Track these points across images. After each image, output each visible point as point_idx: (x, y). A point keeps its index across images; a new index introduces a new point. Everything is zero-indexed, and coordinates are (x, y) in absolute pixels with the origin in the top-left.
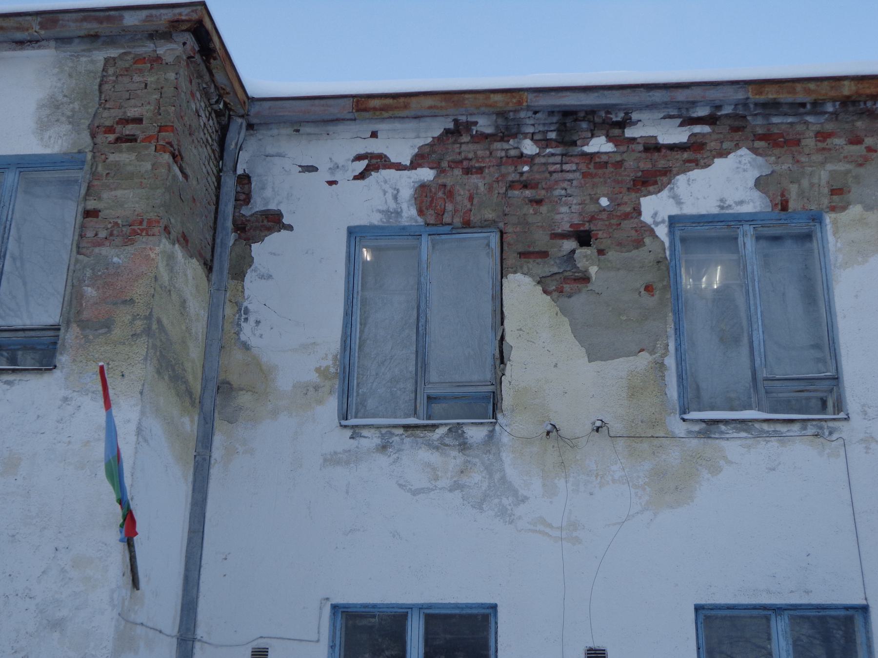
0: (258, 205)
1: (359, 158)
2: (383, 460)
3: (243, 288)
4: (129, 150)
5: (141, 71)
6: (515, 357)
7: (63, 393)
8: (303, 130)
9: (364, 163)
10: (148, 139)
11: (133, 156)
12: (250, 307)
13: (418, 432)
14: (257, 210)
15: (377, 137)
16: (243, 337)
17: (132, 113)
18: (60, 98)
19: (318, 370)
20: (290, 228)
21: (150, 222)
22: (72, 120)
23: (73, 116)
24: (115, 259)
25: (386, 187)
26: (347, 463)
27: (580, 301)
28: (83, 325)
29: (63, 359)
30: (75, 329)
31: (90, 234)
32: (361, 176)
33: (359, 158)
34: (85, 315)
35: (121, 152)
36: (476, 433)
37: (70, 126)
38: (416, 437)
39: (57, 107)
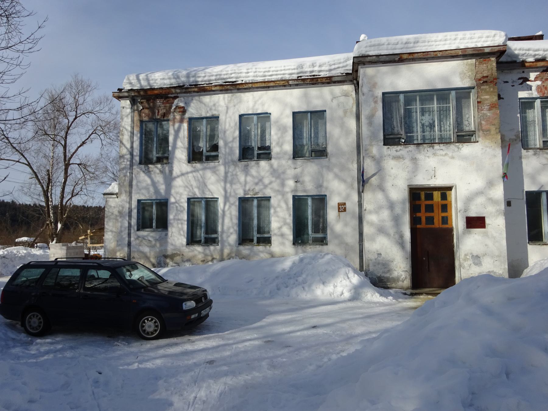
1: (520, 79)
2: (535, 157)
4: (487, 85)
7: (481, 147)
9: (521, 81)
10: (491, 82)
11: (488, 87)
13: (543, 150)
19: (515, 135)
20: (503, 99)
21: (495, 104)
24: (488, 114)
28: (483, 131)
29: (480, 139)
31: (480, 108)
32: (521, 84)
33: (520, 79)
35: (484, 86)
37: (469, 79)
38: (543, 151)
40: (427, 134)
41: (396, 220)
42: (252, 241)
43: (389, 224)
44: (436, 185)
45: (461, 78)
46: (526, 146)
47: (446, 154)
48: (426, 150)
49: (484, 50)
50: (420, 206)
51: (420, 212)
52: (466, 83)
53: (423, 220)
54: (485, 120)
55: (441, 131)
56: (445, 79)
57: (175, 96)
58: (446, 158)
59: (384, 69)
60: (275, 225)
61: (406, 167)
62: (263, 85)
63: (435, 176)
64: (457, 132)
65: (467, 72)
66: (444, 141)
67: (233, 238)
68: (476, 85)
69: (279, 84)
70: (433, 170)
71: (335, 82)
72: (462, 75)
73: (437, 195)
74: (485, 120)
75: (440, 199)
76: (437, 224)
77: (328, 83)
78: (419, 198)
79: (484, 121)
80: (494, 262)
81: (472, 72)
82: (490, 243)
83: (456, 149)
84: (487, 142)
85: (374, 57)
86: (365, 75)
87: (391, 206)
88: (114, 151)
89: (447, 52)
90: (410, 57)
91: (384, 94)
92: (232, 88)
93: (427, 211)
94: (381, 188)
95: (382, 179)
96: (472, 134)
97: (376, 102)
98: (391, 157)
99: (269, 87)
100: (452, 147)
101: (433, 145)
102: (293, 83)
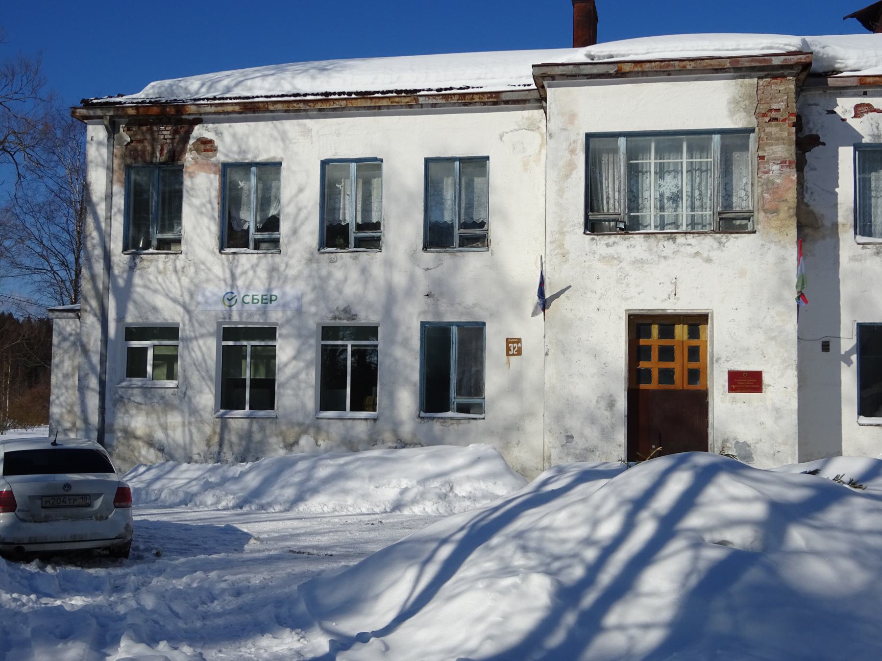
0: (806, 132)
3: (803, 175)
4: (776, 126)
5: (776, 84)
7: (761, 242)
8: (828, 91)
11: (778, 129)
12: (808, 185)
14: (807, 134)
15: (866, 95)
16: (805, 201)
17: (775, 106)
18: (738, 98)
20: (824, 144)
22: (745, 109)
23: (746, 108)
25: (872, 122)
26: (861, 260)
28: (766, 211)
29: (759, 227)
30: (762, 214)
34: (767, 207)
35: (772, 126)
37: (745, 114)
39: (737, 103)
40: (668, 213)
44: (676, 311)
45: (730, 110)
47: (697, 254)
48: (660, 244)
49: (771, 60)
50: (649, 348)
51: (649, 358)
52: (738, 122)
53: (655, 374)
54: (771, 191)
55: (693, 208)
57: (195, 119)
61: (623, 275)
63: (675, 295)
64: (719, 213)
65: (741, 99)
66: (695, 228)
68: (756, 126)
69: (398, 102)
70: (673, 282)
71: (507, 102)
74: (771, 191)
75: (686, 337)
76: (680, 382)
77: (495, 103)
79: (767, 193)
80: (774, 455)
81: (751, 101)
83: (716, 245)
85: (571, 67)
88: (43, 188)
89: (704, 63)
90: (636, 69)
92: (308, 107)
93: (661, 358)
96: (748, 216)
98: (597, 257)
99: (379, 108)
101: (673, 235)
102: (427, 102)
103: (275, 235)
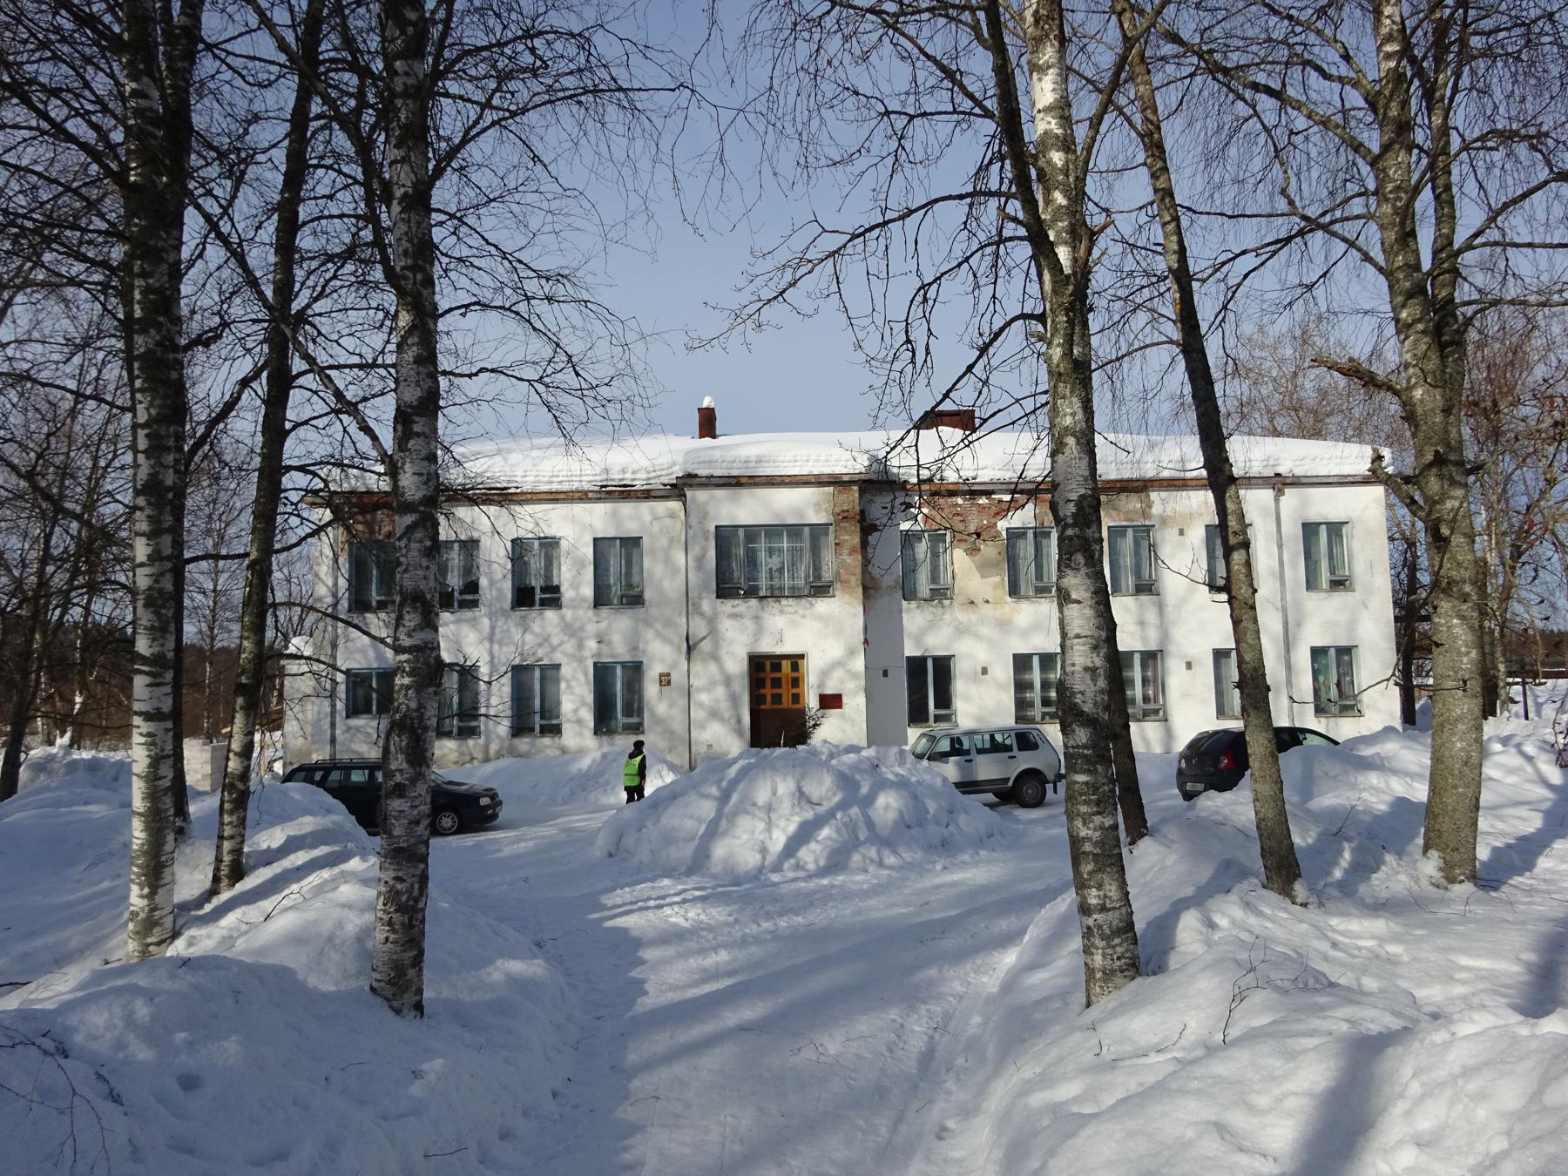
2: (918, 611)
6: (958, 577)
27: (977, 558)
29: (837, 593)
36: (946, 602)
41: (734, 700)
42: (532, 730)
43: (724, 706)
46: (909, 594)
50: (764, 680)
53: (769, 698)
56: (798, 512)
58: (796, 617)
59: (721, 493)
60: (567, 706)
62: (549, 497)
66: (796, 594)
67: (503, 728)
72: (817, 506)
73: (786, 665)
76: (786, 702)
78: (764, 670)
82: (847, 726)
84: (847, 598)
86: (694, 500)
87: (728, 681)
91: (717, 527)
93: (772, 687)
94: (715, 657)
95: (716, 645)
97: (707, 539)
100: (804, 601)
103: (476, 597)
